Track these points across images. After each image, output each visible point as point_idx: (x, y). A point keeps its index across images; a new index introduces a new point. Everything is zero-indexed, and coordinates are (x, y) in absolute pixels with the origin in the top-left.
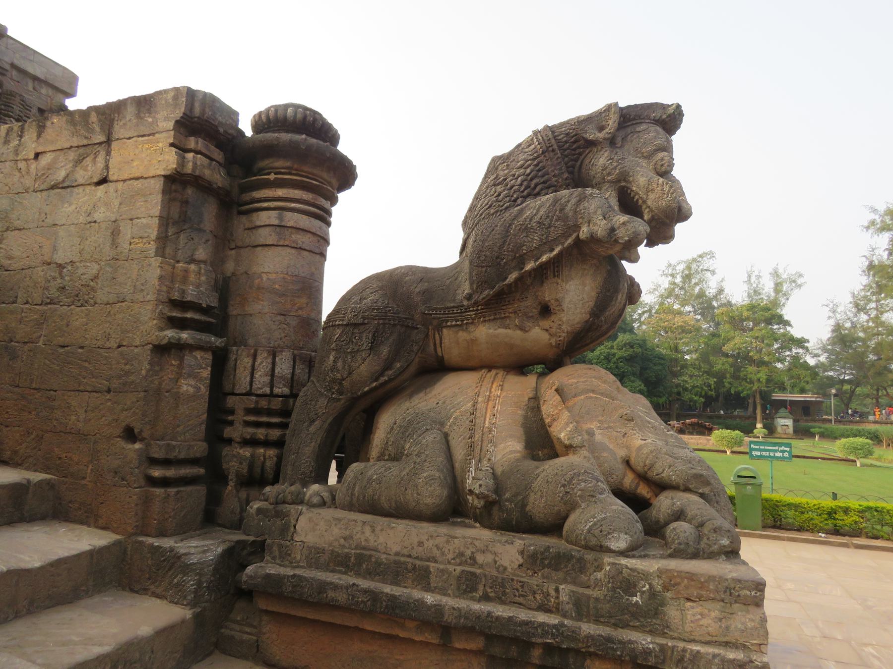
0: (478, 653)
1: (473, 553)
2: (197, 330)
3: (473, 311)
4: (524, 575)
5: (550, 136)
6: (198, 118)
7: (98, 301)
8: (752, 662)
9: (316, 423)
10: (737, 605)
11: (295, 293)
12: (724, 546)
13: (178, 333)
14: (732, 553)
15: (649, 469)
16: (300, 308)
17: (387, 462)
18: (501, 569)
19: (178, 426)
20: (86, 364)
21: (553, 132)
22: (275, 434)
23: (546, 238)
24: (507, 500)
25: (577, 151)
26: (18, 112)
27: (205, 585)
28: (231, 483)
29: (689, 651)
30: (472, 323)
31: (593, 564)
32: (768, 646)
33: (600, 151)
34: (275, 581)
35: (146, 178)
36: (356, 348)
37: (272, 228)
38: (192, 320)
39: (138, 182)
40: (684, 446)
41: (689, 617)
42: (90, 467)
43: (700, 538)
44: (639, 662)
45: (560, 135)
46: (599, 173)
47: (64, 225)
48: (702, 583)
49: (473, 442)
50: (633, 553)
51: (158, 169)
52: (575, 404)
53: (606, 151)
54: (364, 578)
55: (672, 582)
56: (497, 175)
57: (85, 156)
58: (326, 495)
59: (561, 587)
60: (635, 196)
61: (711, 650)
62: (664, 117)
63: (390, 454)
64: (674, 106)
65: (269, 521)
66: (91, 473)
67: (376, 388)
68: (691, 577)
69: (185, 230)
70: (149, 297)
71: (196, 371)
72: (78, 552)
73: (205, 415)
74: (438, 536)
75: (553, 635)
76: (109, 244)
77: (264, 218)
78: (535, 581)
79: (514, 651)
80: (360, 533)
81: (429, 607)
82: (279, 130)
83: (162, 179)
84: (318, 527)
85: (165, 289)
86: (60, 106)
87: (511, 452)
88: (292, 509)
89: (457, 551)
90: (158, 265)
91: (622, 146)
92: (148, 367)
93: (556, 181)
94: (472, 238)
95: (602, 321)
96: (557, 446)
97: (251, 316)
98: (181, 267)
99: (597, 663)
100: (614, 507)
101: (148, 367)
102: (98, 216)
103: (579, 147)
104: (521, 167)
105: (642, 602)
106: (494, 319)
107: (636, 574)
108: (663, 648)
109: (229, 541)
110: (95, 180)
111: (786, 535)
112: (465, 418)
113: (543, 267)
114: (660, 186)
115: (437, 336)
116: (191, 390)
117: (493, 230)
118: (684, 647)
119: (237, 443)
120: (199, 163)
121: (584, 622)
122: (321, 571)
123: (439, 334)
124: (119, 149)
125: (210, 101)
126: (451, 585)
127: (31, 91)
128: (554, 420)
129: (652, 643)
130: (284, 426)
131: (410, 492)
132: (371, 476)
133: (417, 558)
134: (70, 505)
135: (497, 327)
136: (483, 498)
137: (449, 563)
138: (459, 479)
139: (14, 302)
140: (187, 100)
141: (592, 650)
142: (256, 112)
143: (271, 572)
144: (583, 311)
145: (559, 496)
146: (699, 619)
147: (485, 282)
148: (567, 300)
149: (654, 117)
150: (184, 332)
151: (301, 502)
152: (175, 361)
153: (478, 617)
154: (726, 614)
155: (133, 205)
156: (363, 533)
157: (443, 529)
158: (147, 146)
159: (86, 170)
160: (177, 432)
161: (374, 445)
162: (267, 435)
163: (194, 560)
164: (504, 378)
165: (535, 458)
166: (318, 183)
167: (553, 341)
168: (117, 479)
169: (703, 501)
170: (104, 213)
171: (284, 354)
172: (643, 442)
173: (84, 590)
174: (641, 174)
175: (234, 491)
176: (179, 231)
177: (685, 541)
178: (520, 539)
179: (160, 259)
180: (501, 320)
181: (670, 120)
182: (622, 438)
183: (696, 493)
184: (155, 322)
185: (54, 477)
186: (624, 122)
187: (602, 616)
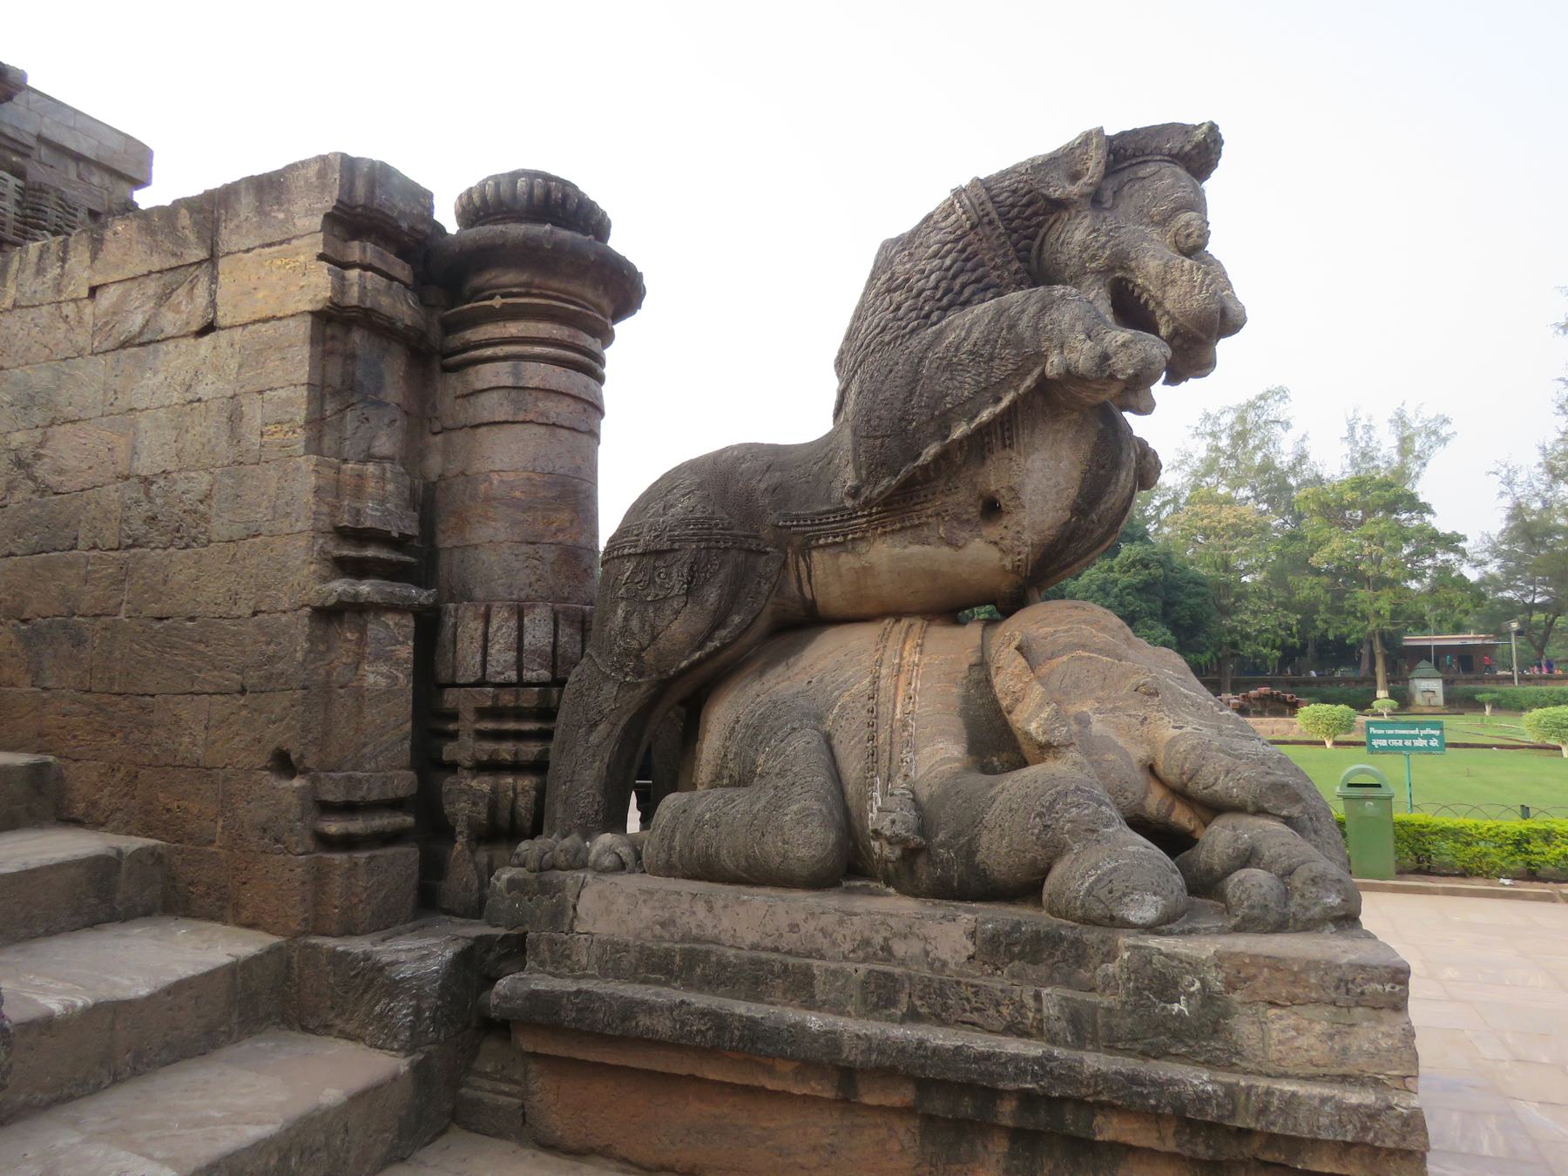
0: (905, 1112)
1: (886, 939)
2: (386, 578)
3: (864, 516)
4: (978, 974)
5: (984, 197)
6: (364, 206)
7: (214, 537)
8: (1390, 1108)
9: (601, 727)
10: (1360, 1009)
12: (1332, 907)
13: (353, 585)
14: (1347, 919)
15: (1190, 779)
16: (559, 530)
17: (728, 789)
18: (937, 964)
19: (365, 745)
20: (201, 647)
21: (988, 189)
22: (531, 750)
23: (986, 380)
24: (942, 845)
25: (1034, 221)
26: (54, 218)
27: (427, 1014)
28: (461, 839)
29: (1277, 1093)
30: (862, 539)
31: (1098, 948)
32: (1419, 1079)
33: (1077, 216)
34: (550, 1001)
35: (280, 319)
36: (662, 594)
37: (501, 392)
38: (376, 560)
39: (268, 325)
40: (1252, 736)
41: (1274, 1034)
42: (220, 823)
43: (1287, 895)
44: (1188, 1115)
45: (1001, 194)
46: (1075, 257)
47: (147, 409)
48: (1295, 974)
49: (876, 747)
50: (1168, 926)
51: (300, 301)
52: (1052, 671)
53: (1086, 217)
54: (700, 990)
55: (1242, 975)
56: (893, 274)
57: (175, 286)
58: (625, 851)
59: (1045, 991)
60: (1142, 293)
61: (1317, 1090)
62: (1188, 147)
63: (731, 776)
64: (1204, 127)
65: (530, 900)
66: (222, 833)
67: (699, 662)
68: (1275, 964)
69: (353, 404)
70: (299, 527)
71: (388, 648)
72: (211, 968)
73: (409, 725)
74: (823, 913)
75: (1034, 1075)
76: (226, 438)
77: (489, 375)
78: (998, 983)
79: (967, 1107)
80: (688, 914)
81: (815, 1037)
82: (503, 219)
83: (309, 318)
84: (614, 907)
85: (325, 509)
86: (125, 204)
87: (944, 761)
88: (570, 878)
89: (859, 938)
90: (311, 468)
91: (1114, 207)
92: (306, 645)
93: (999, 276)
94: (854, 388)
95: (1093, 522)
96: (1025, 747)
97: (476, 549)
98: (352, 469)
99: (1115, 1121)
100: (1131, 849)
101: (306, 645)
102: (204, 390)
103: (1036, 214)
104: (935, 255)
105: (1190, 1012)
106: (902, 529)
107: (1175, 963)
108: (1231, 1091)
109: (463, 937)
110: (195, 328)
111: (1440, 885)
112: (859, 705)
113: (984, 431)
114: (1186, 273)
115: (802, 564)
116: (383, 682)
117: (891, 371)
118: (1268, 1088)
119: (466, 769)
120: (369, 288)
121: (1089, 1051)
122: (624, 983)
123: (805, 560)
124: (231, 272)
125: (380, 175)
126: (851, 996)
127: (74, 182)
128: (1017, 700)
129: (1211, 1082)
130: (546, 736)
131: (771, 840)
132: (702, 814)
133: (789, 953)
134: (191, 889)
135: (906, 543)
136: (897, 843)
137: (846, 958)
138: (854, 813)
140: (341, 176)
141: (1104, 1098)
142: (463, 189)
143: (539, 988)
144: (1059, 505)
145: (1032, 834)
146: (1293, 1038)
147: (883, 464)
148: (1029, 488)
149: (1170, 149)
150: (364, 581)
151: (584, 866)
152: (350, 631)
153: (902, 1050)
154: (1340, 1026)
155: (262, 368)
156: (694, 913)
157: (831, 901)
158: (279, 263)
159: (178, 312)
160: (363, 756)
161: (703, 761)
162: (516, 754)
164: (925, 632)
165: (986, 769)
166: (578, 309)
167: (1008, 563)
168: (266, 840)
169: (1290, 830)
170: (213, 383)
171: (537, 611)
172: (1177, 732)
173: (224, 1032)
174: (1151, 253)
175: (467, 852)
176: (343, 407)
177: (1262, 902)
178: (972, 911)
179: (314, 458)
180: (913, 530)
181: (1198, 153)
183: (1276, 816)
184: (313, 567)
185: (160, 842)
186: (1116, 161)
187: (1119, 1040)
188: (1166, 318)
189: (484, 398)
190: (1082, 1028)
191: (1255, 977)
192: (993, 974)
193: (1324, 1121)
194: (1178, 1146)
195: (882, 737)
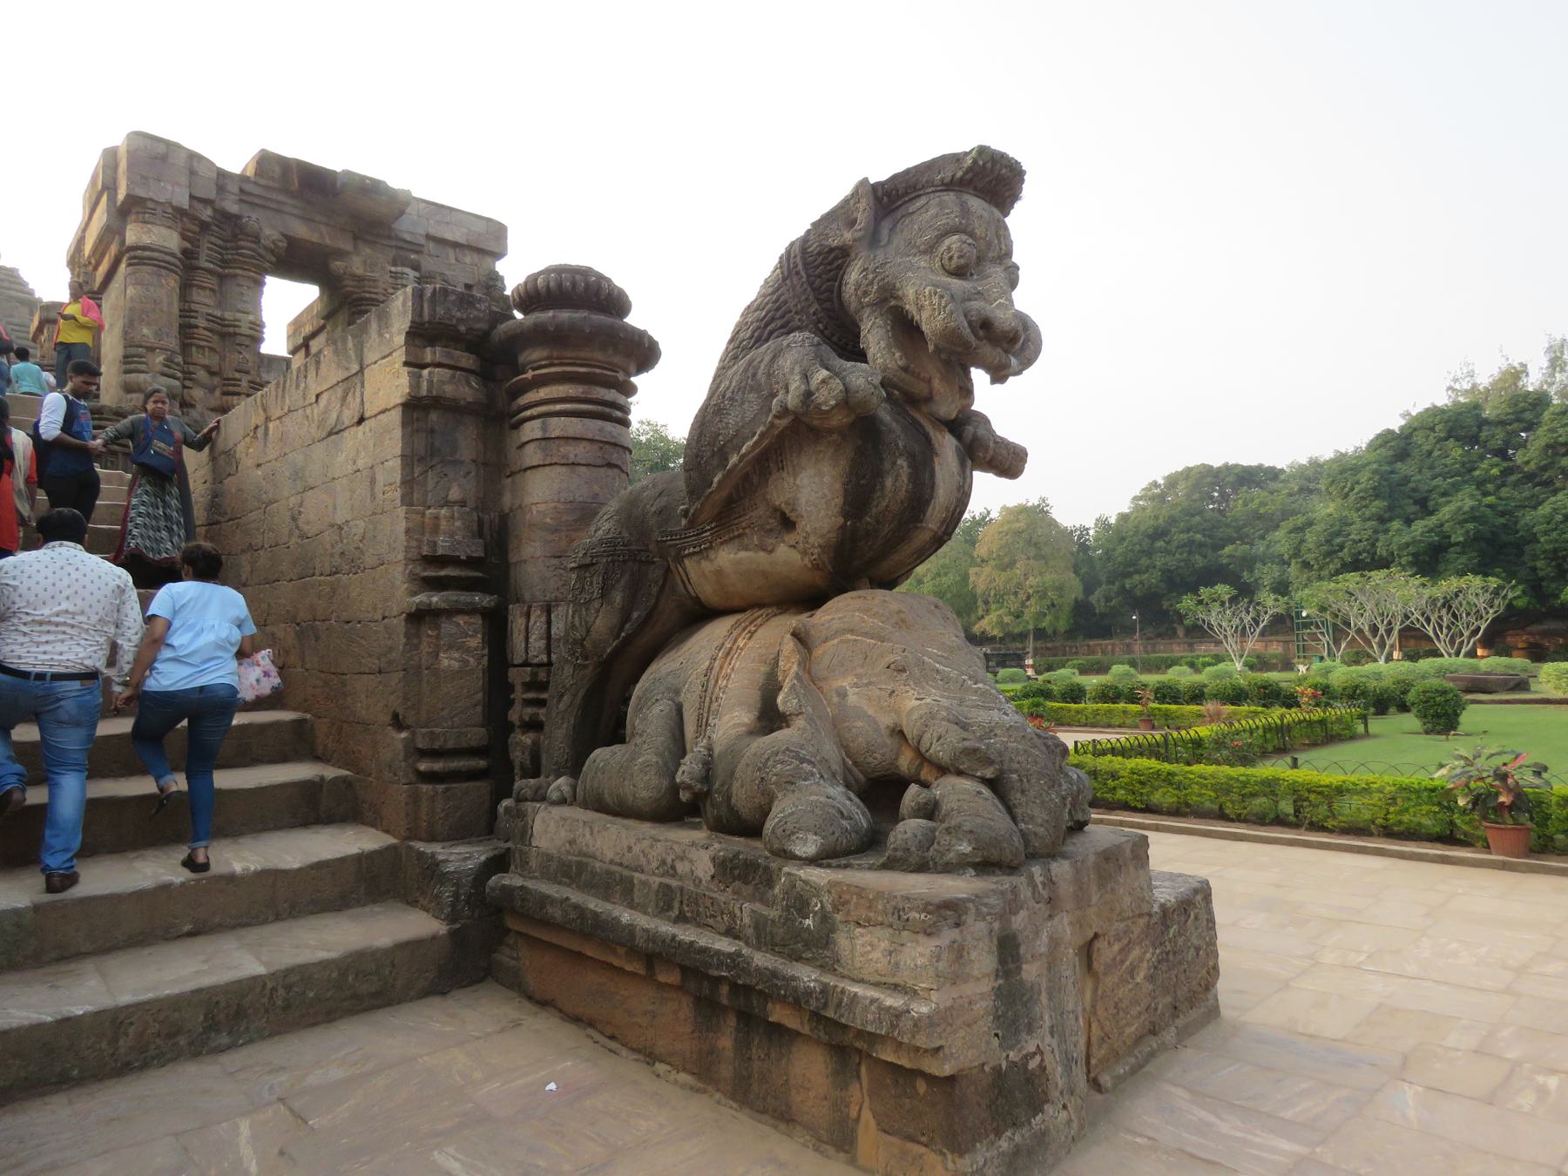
1: (673, 860)
9: (565, 698)
11: (571, 525)
18: (697, 881)
25: (835, 265)
30: (711, 547)
37: (538, 443)
48: (870, 901)
61: (872, 993)
62: (959, 174)
68: (860, 891)
71: (460, 640)
73: (480, 696)
85: (414, 543)
86: (489, 274)
92: (404, 640)
93: (799, 320)
101: (404, 640)
103: (836, 258)
106: (731, 539)
108: (825, 989)
110: (356, 420)
115: (680, 569)
116: (456, 665)
129: (815, 981)
133: (627, 867)
139: (313, 575)
144: (830, 513)
146: (869, 952)
148: (803, 501)
149: (942, 179)
163: (451, 868)
171: (560, 609)
172: (919, 702)
173: (354, 899)
187: (776, 945)
189: (530, 448)
190: (763, 937)
191: (847, 902)
192: (724, 890)
193: (870, 1017)
194: (811, 1030)
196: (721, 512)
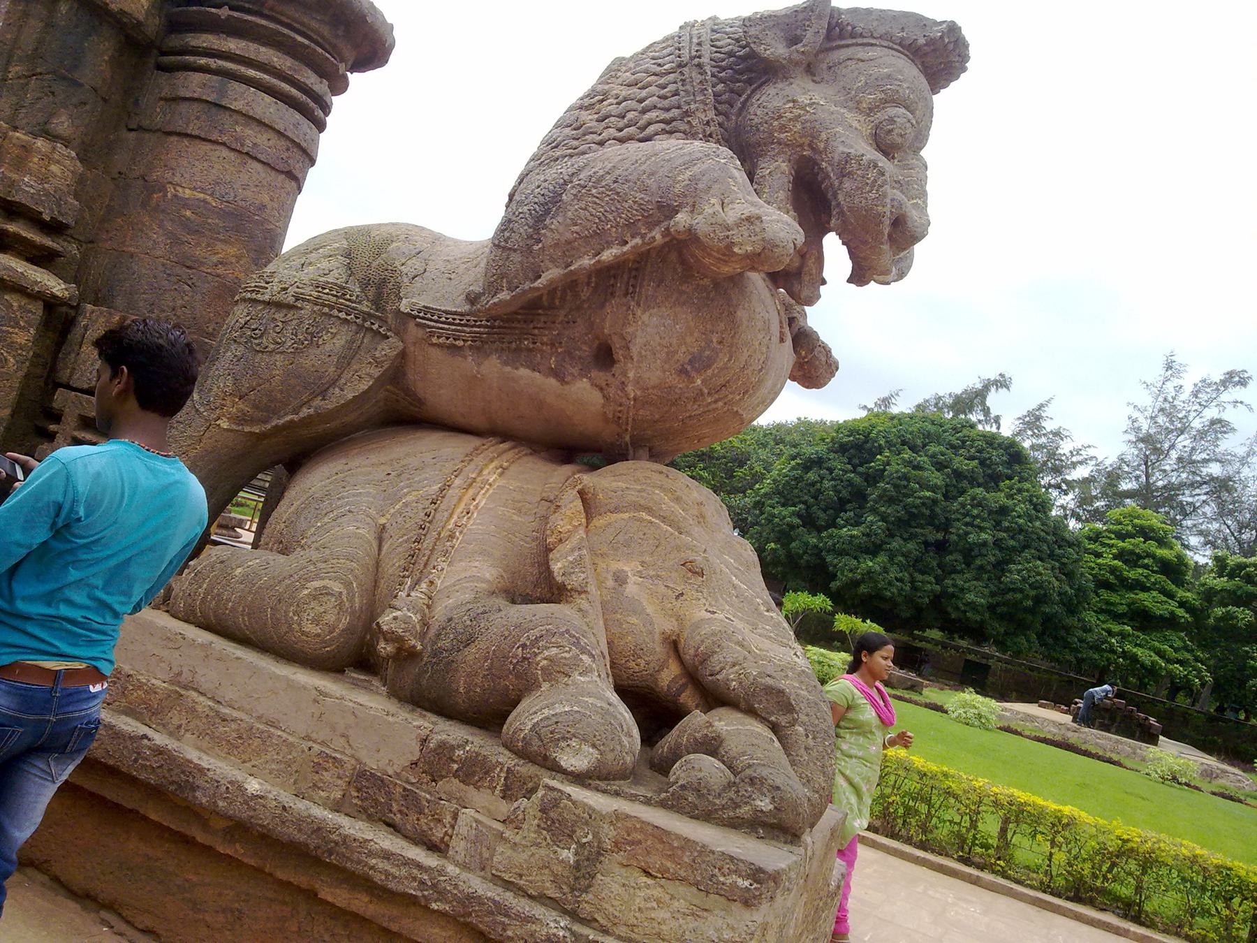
3: (486, 327)
15: (701, 663)
31: (524, 783)
37: (204, 105)
49: (419, 549)
52: (610, 524)
62: (922, 41)
77: (194, 84)
98: (18, 138)
100: (590, 700)
128: (561, 540)
129: (565, 928)
145: (511, 662)
149: (902, 39)
166: (306, 42)
176: (30, 73)
182: (674, 600)
183: (763, 720)
188: (837, 210)
189: (184, 108)
195: (428, 543)
196: (515, 313)
